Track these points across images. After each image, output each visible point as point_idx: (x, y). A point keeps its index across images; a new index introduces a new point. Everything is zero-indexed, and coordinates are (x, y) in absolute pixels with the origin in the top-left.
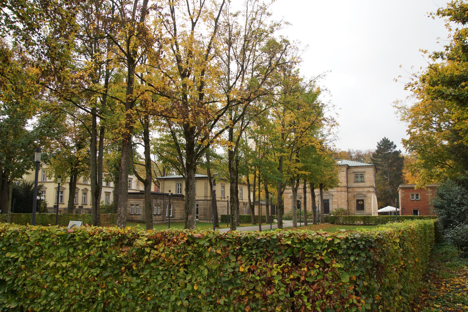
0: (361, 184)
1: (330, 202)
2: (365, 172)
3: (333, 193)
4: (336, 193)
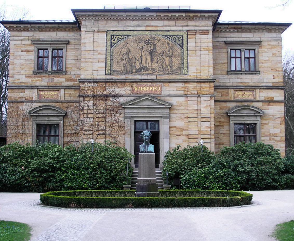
0: (249, 80)
1: (164, 128)
2: (259, 43)
3: (174, 101)
4: (183, 99)
